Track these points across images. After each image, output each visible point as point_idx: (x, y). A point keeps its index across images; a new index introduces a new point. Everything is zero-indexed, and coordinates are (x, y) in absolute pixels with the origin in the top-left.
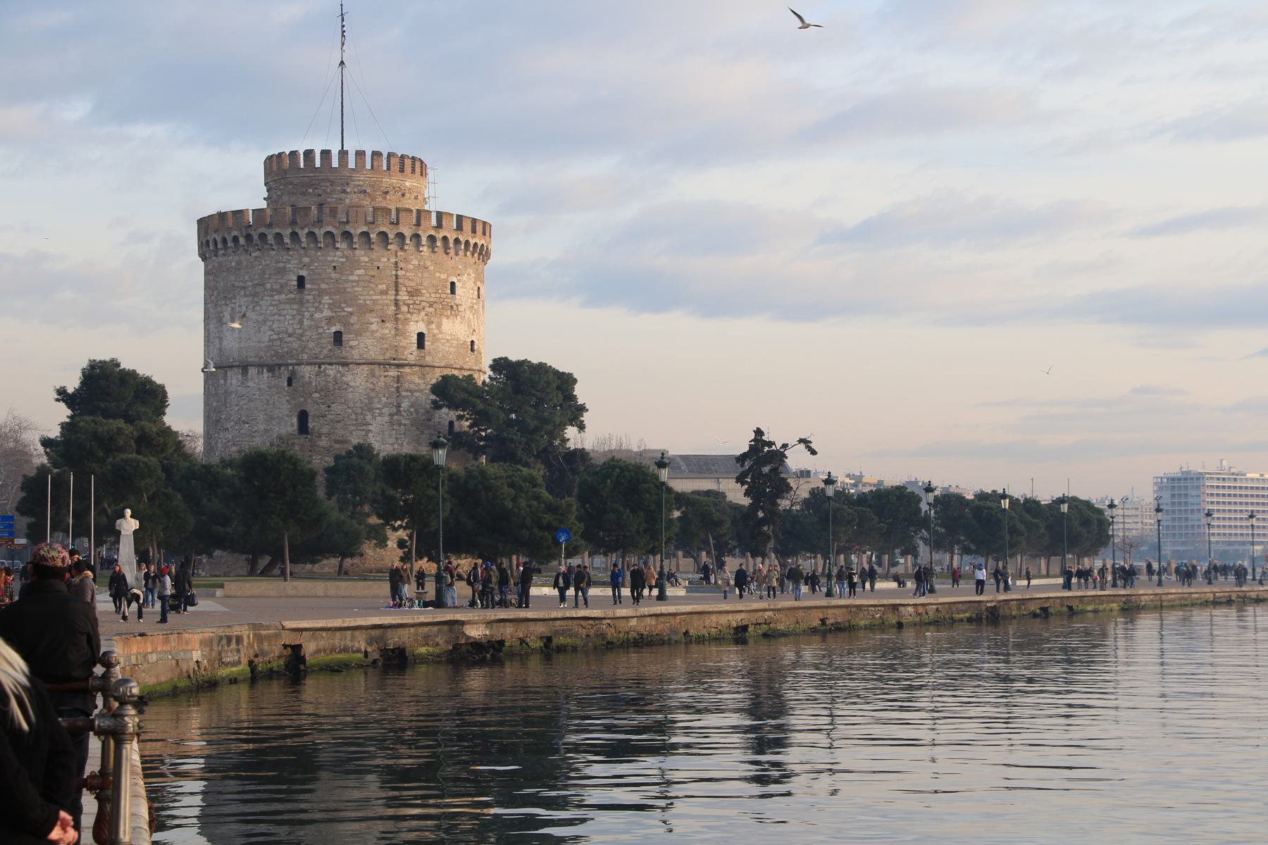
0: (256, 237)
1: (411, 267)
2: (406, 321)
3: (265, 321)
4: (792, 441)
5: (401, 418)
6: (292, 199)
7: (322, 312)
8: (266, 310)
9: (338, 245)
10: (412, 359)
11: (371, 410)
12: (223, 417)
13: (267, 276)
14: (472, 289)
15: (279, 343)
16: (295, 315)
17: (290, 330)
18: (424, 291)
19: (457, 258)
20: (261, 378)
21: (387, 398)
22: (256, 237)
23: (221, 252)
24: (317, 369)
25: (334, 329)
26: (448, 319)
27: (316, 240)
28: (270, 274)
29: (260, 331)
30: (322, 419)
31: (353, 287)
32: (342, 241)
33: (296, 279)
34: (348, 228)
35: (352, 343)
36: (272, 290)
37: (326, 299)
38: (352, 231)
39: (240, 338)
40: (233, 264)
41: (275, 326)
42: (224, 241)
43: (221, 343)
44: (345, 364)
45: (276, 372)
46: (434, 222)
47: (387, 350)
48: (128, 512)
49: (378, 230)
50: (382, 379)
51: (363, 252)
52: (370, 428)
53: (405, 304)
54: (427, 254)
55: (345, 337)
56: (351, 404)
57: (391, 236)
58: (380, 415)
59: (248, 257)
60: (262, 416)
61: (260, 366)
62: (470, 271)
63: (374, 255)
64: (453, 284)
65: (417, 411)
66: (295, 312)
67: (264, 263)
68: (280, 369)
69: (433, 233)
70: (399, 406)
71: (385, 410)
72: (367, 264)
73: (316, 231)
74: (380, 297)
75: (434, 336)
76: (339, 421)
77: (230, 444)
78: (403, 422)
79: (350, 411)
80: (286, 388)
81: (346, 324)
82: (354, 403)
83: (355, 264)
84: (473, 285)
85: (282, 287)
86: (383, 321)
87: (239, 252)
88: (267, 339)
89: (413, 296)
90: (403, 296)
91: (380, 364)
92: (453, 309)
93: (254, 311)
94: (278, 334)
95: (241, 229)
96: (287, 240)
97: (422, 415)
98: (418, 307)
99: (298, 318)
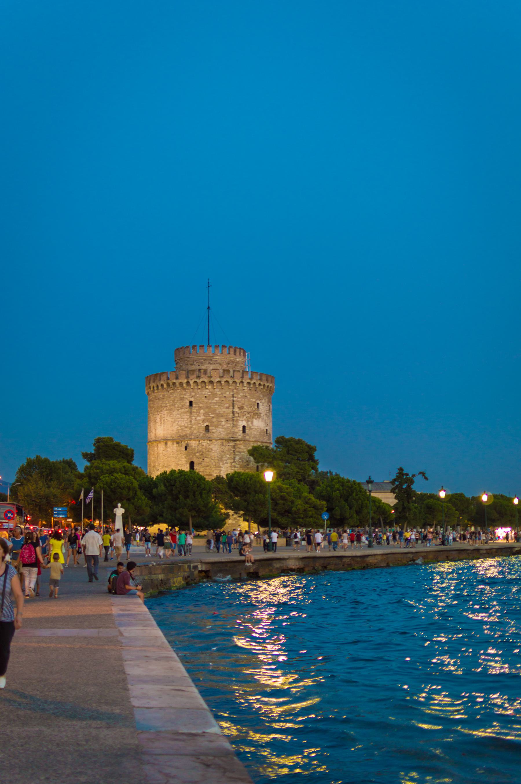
0: (171, 384)
1: (240, 396)
2: (237, 421)
3: (175, 421)
4: (416, 473)
5: (235, 464)
6: (187, 367)
7: (200, 417)
9: (207, 387)
10: (240, 437)
11: (222, 460)
12: (157, 464)
13: (176, 401)
14: (267, 406)
15: (181, 431)
17: (186, 425)
18: (245, 407)
19: (260, 392)
21: (229, 455)
22: (171, 384)
23: (156, 391)
24: (198, 442)
25: (205, 425)
26: (256, 419)
27: (198, 385)
28: (177, 400)
29: (172, 426)
30: (200, 466)
31: (214, 405)
32: (209, 385)
33: (188, 402)
34: (211, 379)
35: (214, 431)
36: (178, 407)
37: (202, 411)
38: (213, 381)
40: (161, 396)
41: (180, 423)
42: (158, 386)
43: (155, 432)
44: (210, 440)
45: (180, 444)
46: (250, 376)
47: (229, 433)
48: (119, 505)
49: (225, 380)
50: (227, 447)
51: (218, 390)
52: (222, 469)
53: (237, 413)
54: (246, 390)
55: (210, 428)
56: (213, 458)
57: (231, 382)
58: (226, 463)
59: (168, 393)
61: (173, 440)
62: (265, 398)
63: (223, 391)
64: (258, 404)
65: (243, 461)
66: (188, 417)
68: (181, 442)
69: (249, 381)
70: (234, 459)
71: (229, 461)
72: (221, 395)
73: (197, 380)
74: (225, 410)
75: (250, 427)
76: (208, 466)
78: (237, 466)
79: (212, 461)
80: (185, 451)
81: (211, 422)
82: (215, 458)
83: (214, 395)
84: (267, 405)
85: (183, 406)
86: (227, 421)
87: (163, 391)
88: (176, 429)
89: (240, 409)
90: (236, 409)
91: (226, 440)
92: (258, 415)
96: (185, 385)
97: (245, 463)
98: (243, 414)
99: (189, 419)
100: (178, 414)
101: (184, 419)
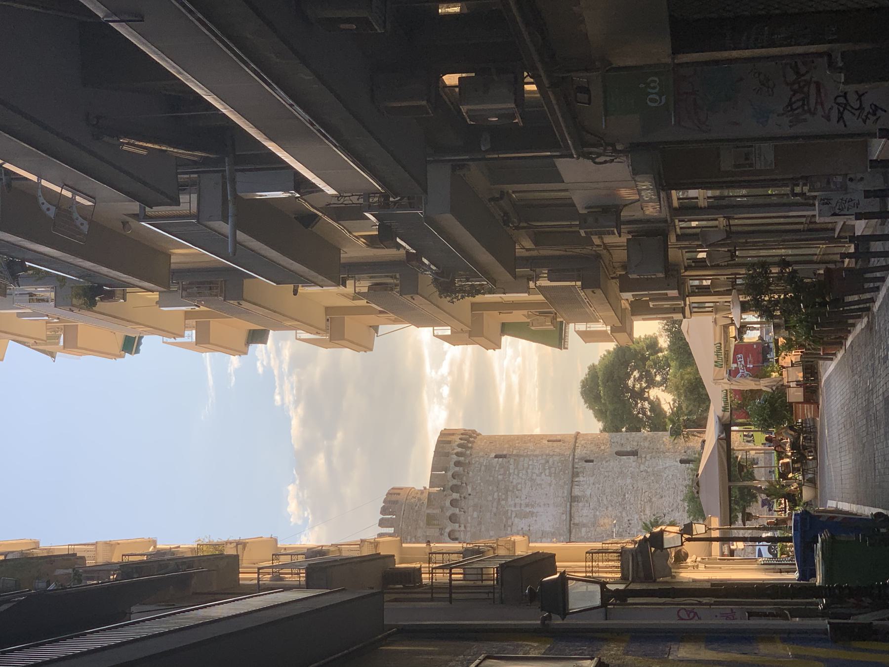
0: (455, 482)
3: (532, 480)
8: (522, 479)
13: (491, 479)
16: (530, 460)
20: (583, 483)
28: (490, 476)
29: (541, 485)
36: (504, 474)
39: (544, 505)
40: (475, 514)
41: (537, 471)
42: (453, 519)
45: (579, 470)
60: (619, 481)
66: (527, 459)
67: (479, 481)
68: (577, 468)
77: (643, 517)
80: (595, 463)
88: (549, 478)
93: (521, 490)
94: (545, 470)
95: (446, 496)
100: (518, 475)
101: (529, 465)
